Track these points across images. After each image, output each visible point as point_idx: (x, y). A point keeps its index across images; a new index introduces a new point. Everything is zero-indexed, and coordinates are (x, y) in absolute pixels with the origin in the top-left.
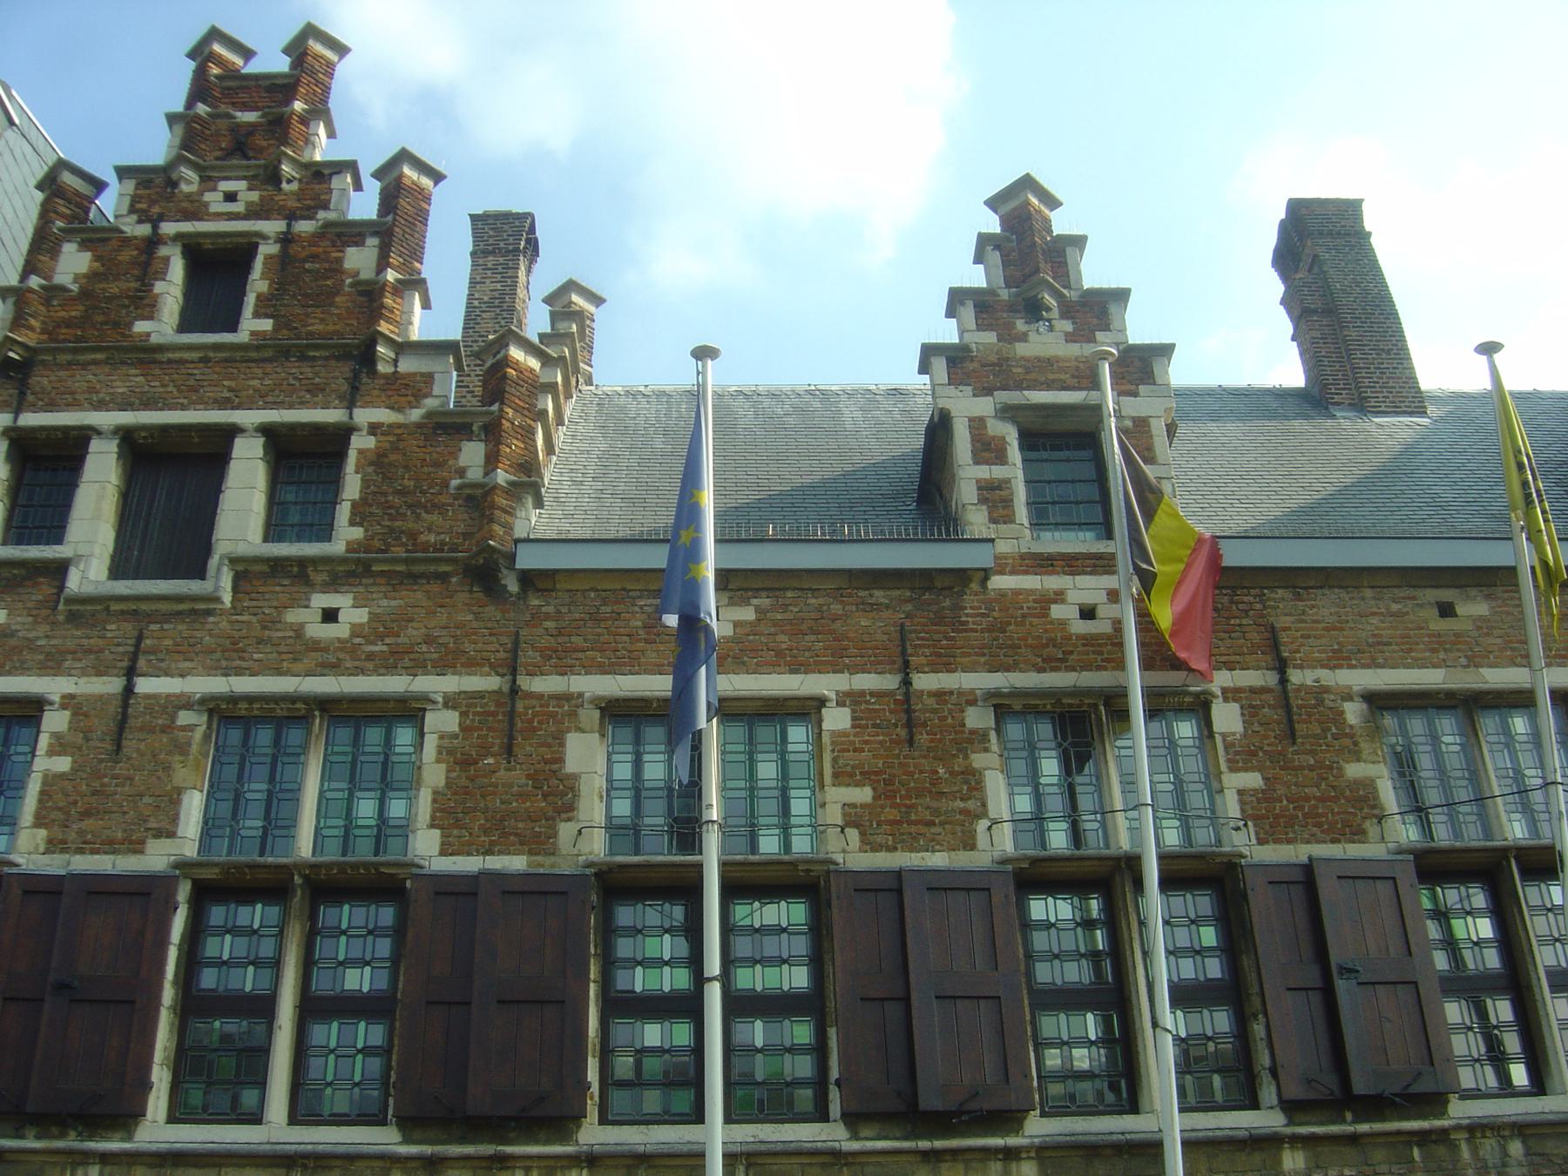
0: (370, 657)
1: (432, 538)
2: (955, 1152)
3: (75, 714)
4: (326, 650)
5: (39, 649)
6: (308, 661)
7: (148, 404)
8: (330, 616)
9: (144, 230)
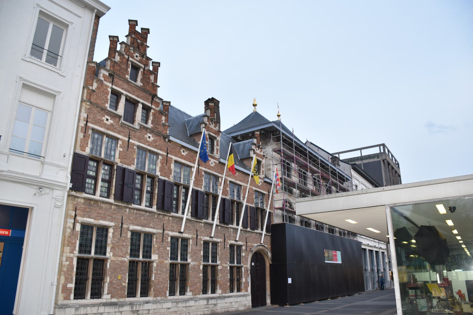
0: (153, 145)
1: (159, 130)
2: (198, 222)
3: (122, 142)
4: (149, 142)
5: (117, 129)
6: (147, 144)
7: (128, 92)
8: (149, 137)
9: (126, 57)
